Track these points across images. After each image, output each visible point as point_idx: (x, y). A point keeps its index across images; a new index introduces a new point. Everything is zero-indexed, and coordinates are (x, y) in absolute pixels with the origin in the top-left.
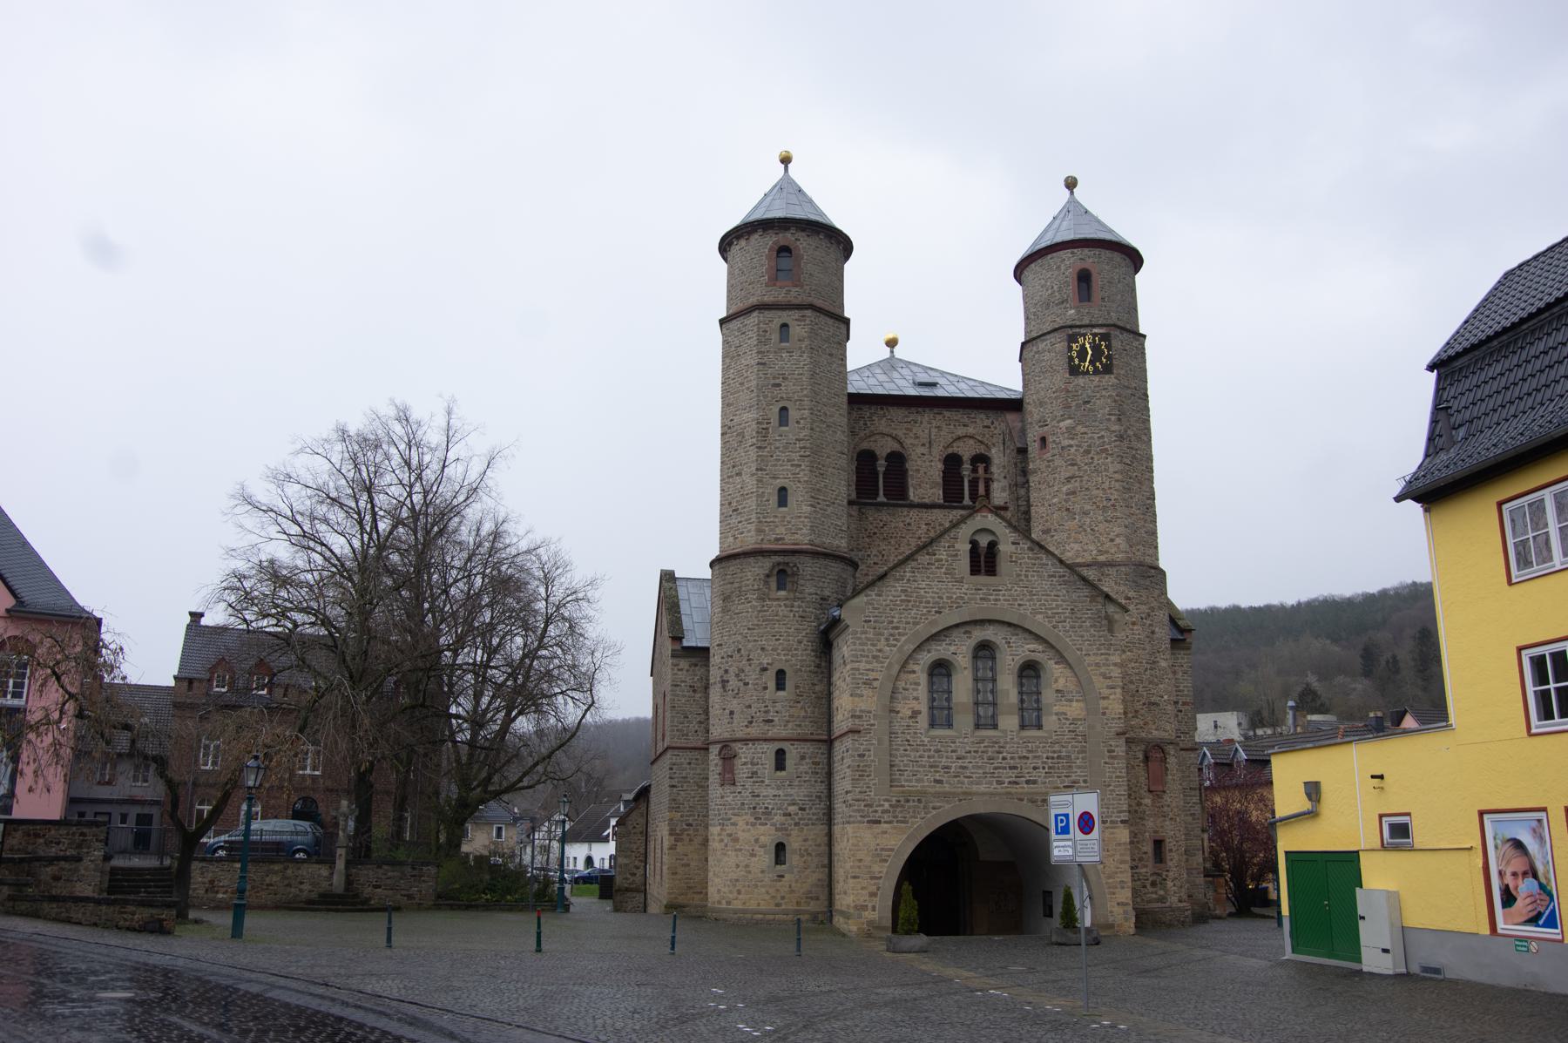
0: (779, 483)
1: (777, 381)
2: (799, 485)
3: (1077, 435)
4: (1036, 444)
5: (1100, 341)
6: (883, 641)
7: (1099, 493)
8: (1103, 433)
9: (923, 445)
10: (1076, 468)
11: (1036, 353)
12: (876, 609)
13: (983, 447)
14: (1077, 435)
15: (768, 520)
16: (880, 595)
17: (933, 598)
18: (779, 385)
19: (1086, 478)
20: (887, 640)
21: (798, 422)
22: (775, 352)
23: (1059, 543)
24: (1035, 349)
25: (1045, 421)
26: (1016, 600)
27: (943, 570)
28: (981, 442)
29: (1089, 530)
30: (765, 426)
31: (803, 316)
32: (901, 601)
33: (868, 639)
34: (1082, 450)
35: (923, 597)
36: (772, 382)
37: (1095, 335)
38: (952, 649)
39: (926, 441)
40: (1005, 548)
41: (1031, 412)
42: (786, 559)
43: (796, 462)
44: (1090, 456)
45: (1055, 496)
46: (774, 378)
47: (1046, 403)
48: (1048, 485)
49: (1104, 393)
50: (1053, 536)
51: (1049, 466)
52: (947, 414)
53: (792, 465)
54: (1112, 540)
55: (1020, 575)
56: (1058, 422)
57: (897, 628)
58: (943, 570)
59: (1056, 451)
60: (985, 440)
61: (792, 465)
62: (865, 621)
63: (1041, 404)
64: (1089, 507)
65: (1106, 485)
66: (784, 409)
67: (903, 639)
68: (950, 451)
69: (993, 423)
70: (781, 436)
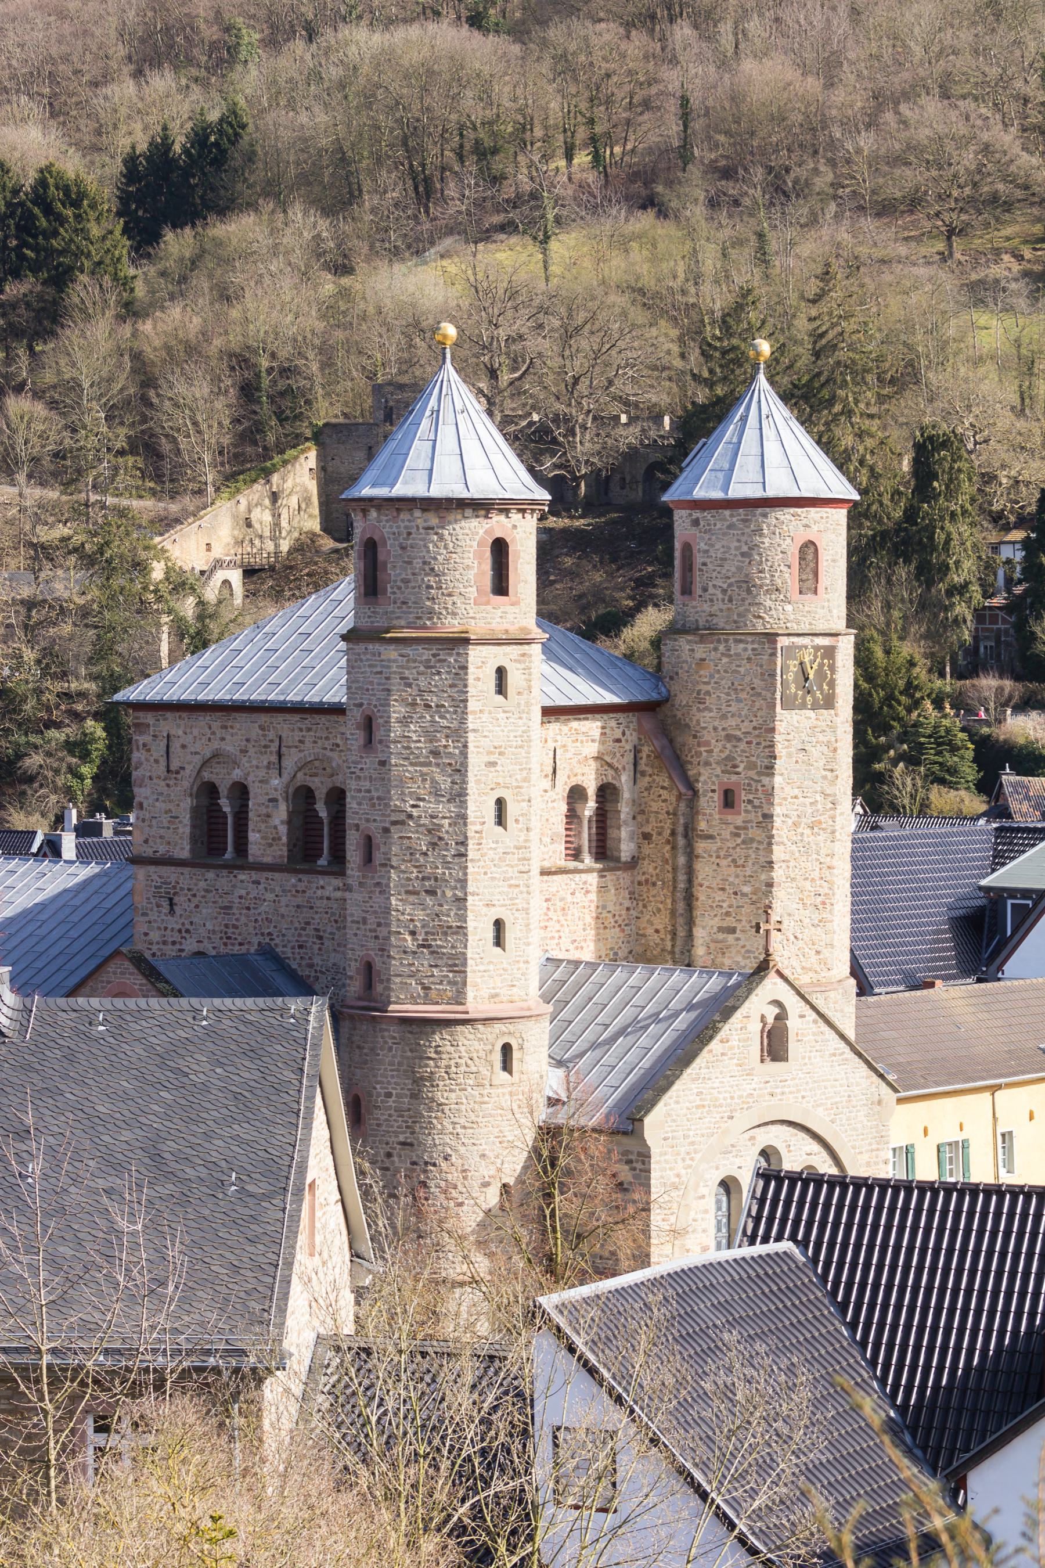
0: (495, 914)
1: (492, 759)
2: (517, 914)
3: (785, 799)
4: (716, 796)
5: (822, 659)
6: (679, 1161)
7: (808, 884)
8: (818, 798)
9: (546, 776)
10: (782, 847)
11: (723, 654)
12: (674, 1121)
13: (611, 772)
14: (785, 799)
15: (482, 968)
16: (677, 1102)
17: (725, 1099)
18: (493, 764)
19: (791, 864)
20: (683, 1160)
21: (517, 821)
22: (490, 713)
23: (748, 951)
24: (722, 647)
25: (735, 766)
26: (799, 1091)
27: (735, 1061)
28: (609, 765)
29: (792, 938)
30: (478, 828)
31: (523, 655)
32: (698, 1107)
33: (666, 1162)
34: (790, 822)
35: (716, 1099)
36: (486, 759)
37: (817, 648)
38: (738, 1161)
39: (550, 770)
40: (793, 1023)
41: (707, 743)
42: (511, 1027)
43: (513, 882)
44: (799, 830)
45: (745, 883)
46: (489, 753)
47: (739, 740)
48: (734, 861)
49: (821, 737)
50: (738, 939)
51: (738, 835)
52: (575, 724)
53: (510, 886)
54: (818, 952)
55: (803, 1058)
56: (760, 774)
57: (693, 1143)
58: (735, 1061)
59: (751, 816)
60: (614, 761)
61: (510, 886)
62: (665, 1139)
63: (729, 738)
64: (795, 906)
65: (816, 875)
66: (500, 803)
67: (698, 1156)
68: (574, 781)
69: (624, 734)
70: (497, 842)
